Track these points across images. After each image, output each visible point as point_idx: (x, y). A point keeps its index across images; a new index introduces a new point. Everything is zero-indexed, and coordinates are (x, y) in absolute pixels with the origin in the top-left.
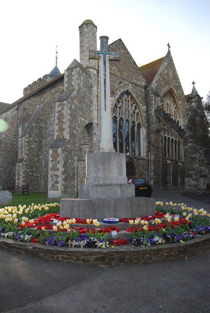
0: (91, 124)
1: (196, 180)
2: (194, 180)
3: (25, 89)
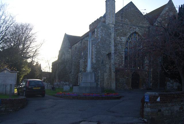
0: (111, 53)
1: (172, 83)
2: (171, 83)
3: (90, 26)
